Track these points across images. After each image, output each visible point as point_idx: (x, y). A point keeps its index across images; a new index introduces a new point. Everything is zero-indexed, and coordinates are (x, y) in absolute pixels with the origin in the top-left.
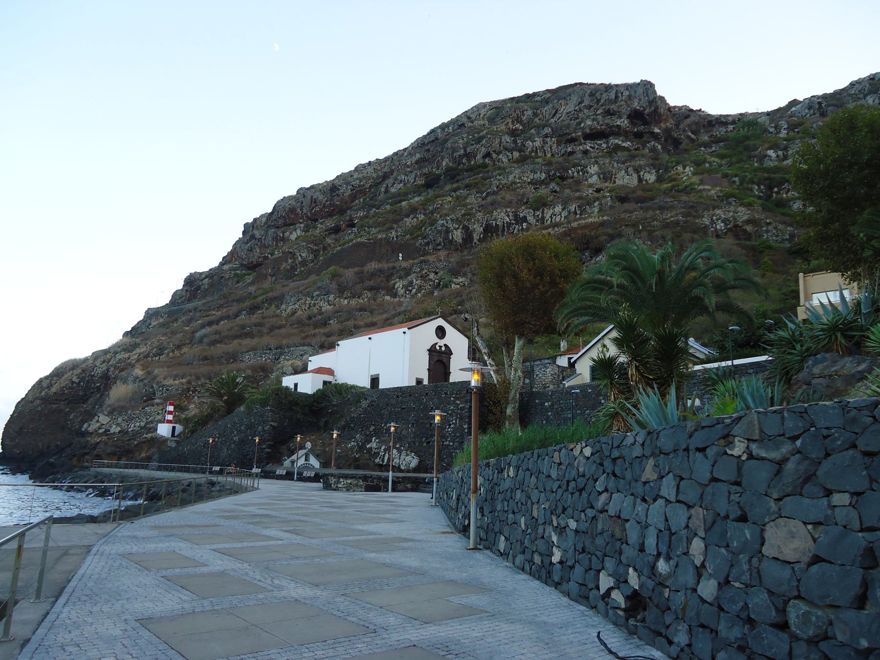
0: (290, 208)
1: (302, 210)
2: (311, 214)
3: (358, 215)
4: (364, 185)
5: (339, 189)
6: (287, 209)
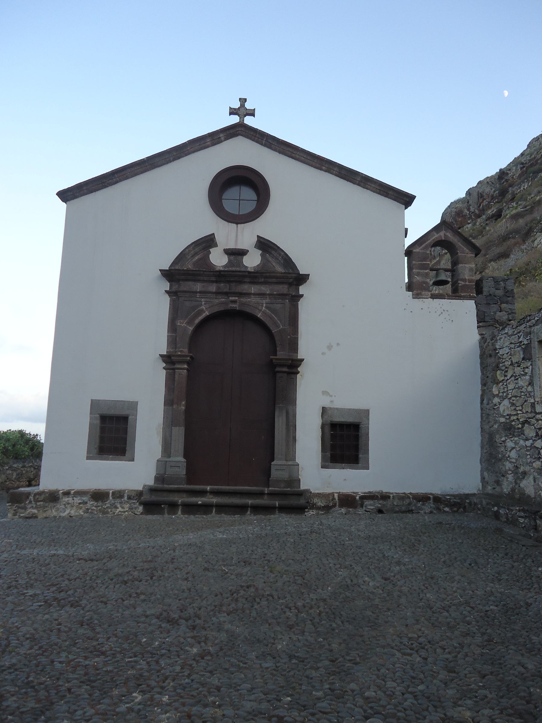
0: (456, 212)
1: (469, 209)
2: (480, 210)
3: (522, 188)
4: (535, 158)
5: (507, 174)
6: (453, 214)
